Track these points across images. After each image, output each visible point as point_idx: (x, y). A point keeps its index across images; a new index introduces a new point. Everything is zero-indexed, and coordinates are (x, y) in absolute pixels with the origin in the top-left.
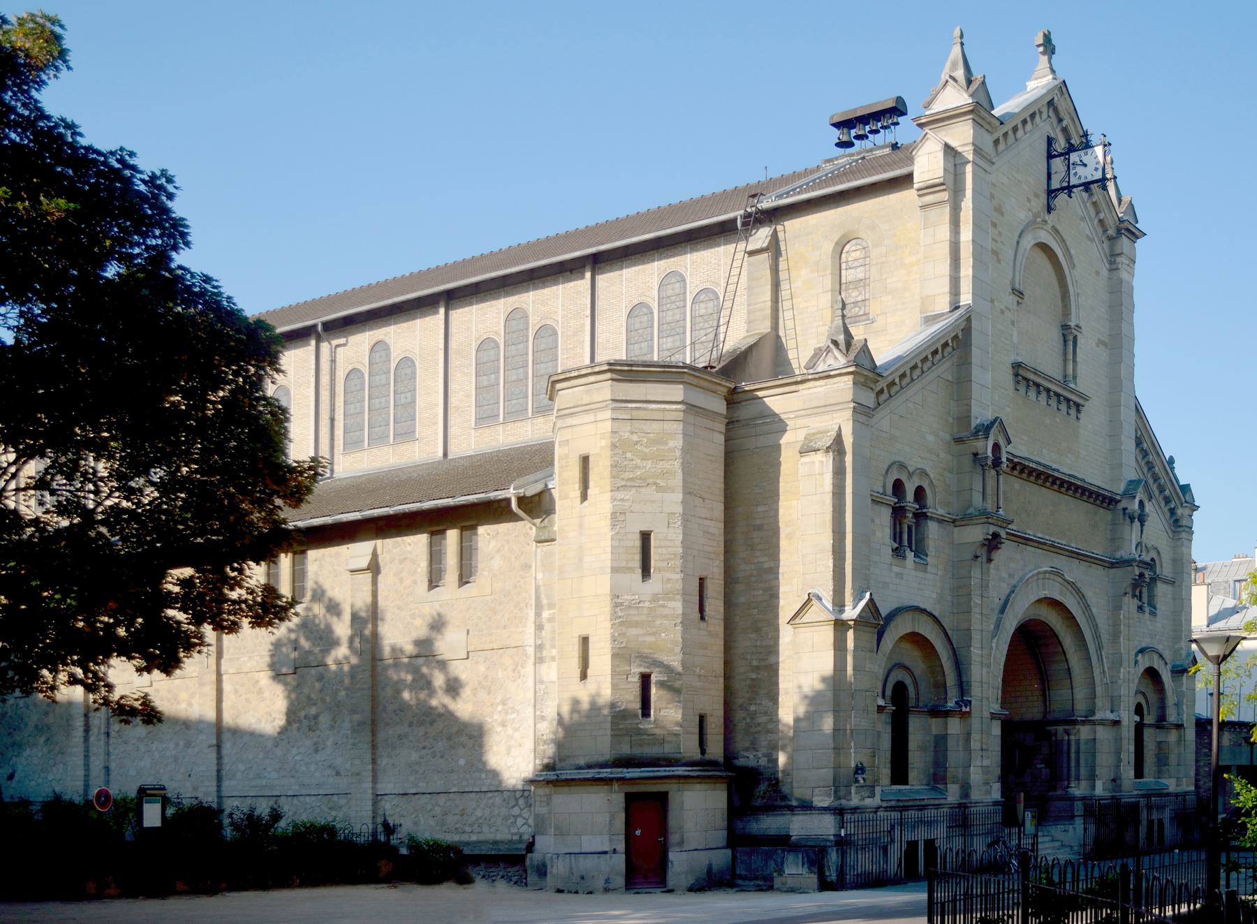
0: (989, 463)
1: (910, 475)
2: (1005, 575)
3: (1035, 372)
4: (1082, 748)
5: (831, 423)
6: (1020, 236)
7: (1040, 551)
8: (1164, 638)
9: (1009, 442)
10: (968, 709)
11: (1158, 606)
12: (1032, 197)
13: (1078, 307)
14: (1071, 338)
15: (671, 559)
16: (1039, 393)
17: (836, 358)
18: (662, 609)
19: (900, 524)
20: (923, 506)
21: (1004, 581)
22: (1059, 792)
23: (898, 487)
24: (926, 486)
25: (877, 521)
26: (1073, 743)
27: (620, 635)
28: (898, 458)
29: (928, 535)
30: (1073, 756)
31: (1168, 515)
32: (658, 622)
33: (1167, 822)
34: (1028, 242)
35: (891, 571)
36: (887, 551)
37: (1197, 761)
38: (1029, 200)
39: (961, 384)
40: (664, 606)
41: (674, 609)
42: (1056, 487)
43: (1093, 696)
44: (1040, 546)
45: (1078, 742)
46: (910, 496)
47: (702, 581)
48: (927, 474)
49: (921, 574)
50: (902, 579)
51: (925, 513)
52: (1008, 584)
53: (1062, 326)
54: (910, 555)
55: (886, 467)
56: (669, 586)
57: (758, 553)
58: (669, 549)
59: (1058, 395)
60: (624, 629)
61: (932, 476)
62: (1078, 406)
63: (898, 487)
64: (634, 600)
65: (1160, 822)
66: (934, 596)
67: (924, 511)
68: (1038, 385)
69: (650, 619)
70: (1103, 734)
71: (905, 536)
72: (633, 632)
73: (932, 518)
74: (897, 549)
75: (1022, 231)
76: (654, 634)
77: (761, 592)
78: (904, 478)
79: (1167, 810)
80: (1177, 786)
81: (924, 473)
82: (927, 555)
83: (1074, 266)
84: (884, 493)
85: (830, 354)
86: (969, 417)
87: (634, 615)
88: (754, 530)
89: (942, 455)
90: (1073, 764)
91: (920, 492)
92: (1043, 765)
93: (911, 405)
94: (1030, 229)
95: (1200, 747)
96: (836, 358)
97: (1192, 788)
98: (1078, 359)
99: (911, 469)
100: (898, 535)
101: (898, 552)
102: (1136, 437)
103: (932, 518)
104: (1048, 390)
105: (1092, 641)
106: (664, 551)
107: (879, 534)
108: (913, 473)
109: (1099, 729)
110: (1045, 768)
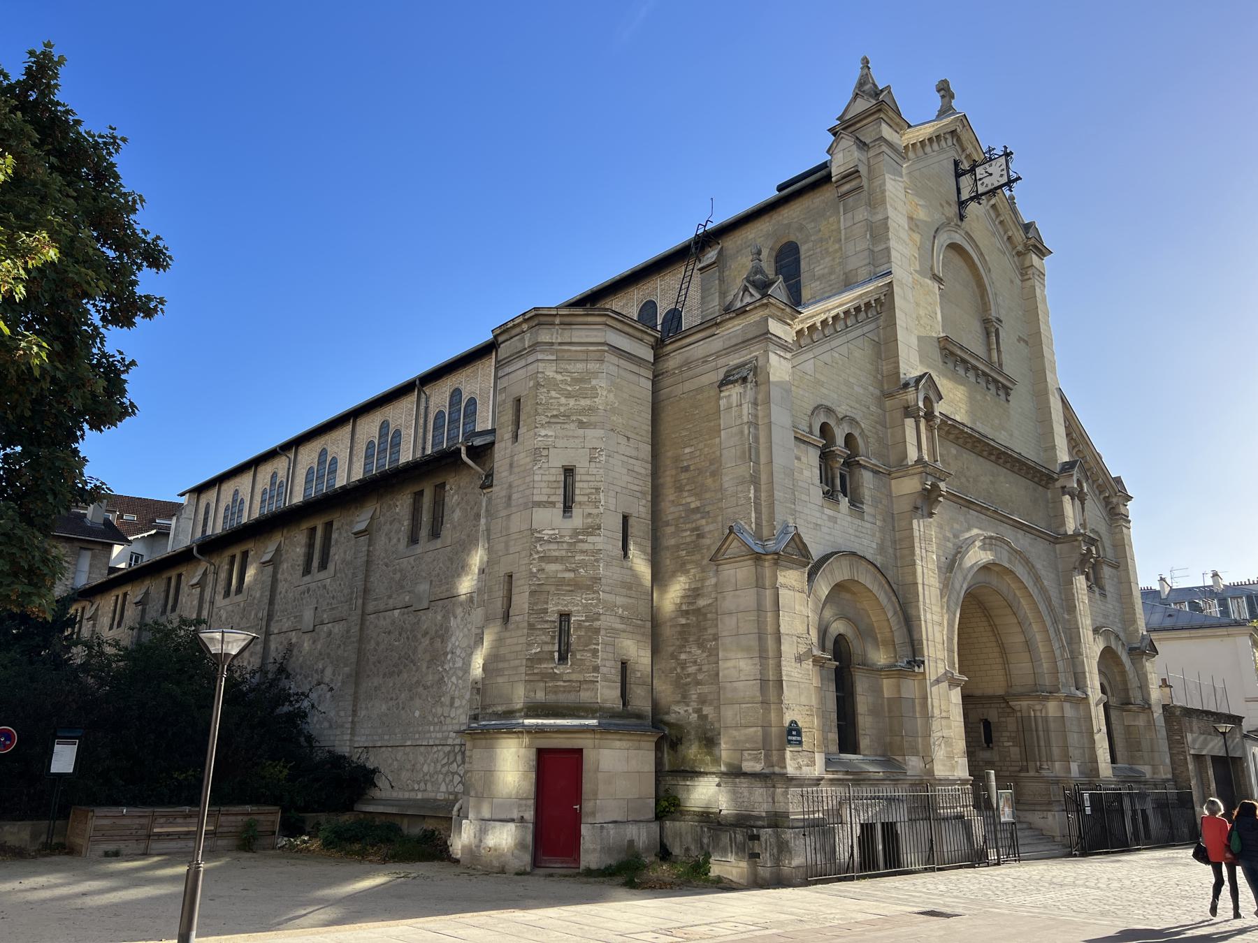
0: (921, 414)
2: (949, 535)
3: (962, 348)
4: (1052, 725)
5: (749, 357)
6: (936, 232)
7: (984, 517)
8: (1117, 620)
9: (941, 398)
10: (921, 670)
11: (1107, 588)
12: (945, 204)
13: (997, 304)
14: (993, 330)
15: (592, 494)
16: (967, 370)
17: (752, 295)
18: (580, 544)
19: (831, 470)
21: (949, 541)
22: (1032, 773)
23: (825, 430)
24: (856, 434)
25: (804, 459)
26: (1040, 720)
27: (539, 570)
30: (1041, 733)
31: (1104, 504)
32: (577, 558)
33: (1150, 812)
34: (944, 239)
35: (823, 513)
36: (817, 492)
37: (1170, 749)
38: (942, 206)
39: (885, 347)
40: (582, 541)
41: (594, 544)
42: (993, 458)
43: (1055, 672)
44: (983, 511)
45: (1046, 719)
46: (840, 441)
47: (625, 519)
48: (857, 422)
49: (858, 522)
50: (836, 523)
52: (954, 545)
54: (844, 502)
55: (811, 408)
56: (590, 520)
57: (686, 494)
58: (590, 483)
59: (985, 374)
60: (543, 565)
61: (863, 425)
62: (1006, 388)
63: (825, 430)
64: (554, 534)
65: (1143, 811)
66: (874, 546)
67: (857, 459)
68: (964, 361)
69: (570, 554)
70: (1069, 711)
71: (838, 482)
72: (552, 568)
73: (865, 467)
74: (828, 492)
75: (938, 229)
76: (573, 571)
77: (688, 533)
78: (832, 423)
79: (1149, 799)
80: (1154, 774)
81: (852, 421)
82: (862, 503)
83: (990, 271)
84: (811, 433)
85: (746, 293)
86: (898, 373)
87: (554, 550)
88: (682, 472)
89: (873, 408)
90: (1042, 743)
91: (849, 439)
92: (1011, 744)
93: (836, 355)
94: (945, 229)
95: (1171, 733)
96: (752, 295)
97: (1169, 776)
98: (1002, 349)
99: (840, 416)
100: (830, 480)
101: (830, 495)
103: (865, 467)
104: (975, 368)
105: (1047, 613)
106: (585, 485)
107: (807, 473)
108: (842, 419)
109: (1067, 706)
110: (1013, 746)
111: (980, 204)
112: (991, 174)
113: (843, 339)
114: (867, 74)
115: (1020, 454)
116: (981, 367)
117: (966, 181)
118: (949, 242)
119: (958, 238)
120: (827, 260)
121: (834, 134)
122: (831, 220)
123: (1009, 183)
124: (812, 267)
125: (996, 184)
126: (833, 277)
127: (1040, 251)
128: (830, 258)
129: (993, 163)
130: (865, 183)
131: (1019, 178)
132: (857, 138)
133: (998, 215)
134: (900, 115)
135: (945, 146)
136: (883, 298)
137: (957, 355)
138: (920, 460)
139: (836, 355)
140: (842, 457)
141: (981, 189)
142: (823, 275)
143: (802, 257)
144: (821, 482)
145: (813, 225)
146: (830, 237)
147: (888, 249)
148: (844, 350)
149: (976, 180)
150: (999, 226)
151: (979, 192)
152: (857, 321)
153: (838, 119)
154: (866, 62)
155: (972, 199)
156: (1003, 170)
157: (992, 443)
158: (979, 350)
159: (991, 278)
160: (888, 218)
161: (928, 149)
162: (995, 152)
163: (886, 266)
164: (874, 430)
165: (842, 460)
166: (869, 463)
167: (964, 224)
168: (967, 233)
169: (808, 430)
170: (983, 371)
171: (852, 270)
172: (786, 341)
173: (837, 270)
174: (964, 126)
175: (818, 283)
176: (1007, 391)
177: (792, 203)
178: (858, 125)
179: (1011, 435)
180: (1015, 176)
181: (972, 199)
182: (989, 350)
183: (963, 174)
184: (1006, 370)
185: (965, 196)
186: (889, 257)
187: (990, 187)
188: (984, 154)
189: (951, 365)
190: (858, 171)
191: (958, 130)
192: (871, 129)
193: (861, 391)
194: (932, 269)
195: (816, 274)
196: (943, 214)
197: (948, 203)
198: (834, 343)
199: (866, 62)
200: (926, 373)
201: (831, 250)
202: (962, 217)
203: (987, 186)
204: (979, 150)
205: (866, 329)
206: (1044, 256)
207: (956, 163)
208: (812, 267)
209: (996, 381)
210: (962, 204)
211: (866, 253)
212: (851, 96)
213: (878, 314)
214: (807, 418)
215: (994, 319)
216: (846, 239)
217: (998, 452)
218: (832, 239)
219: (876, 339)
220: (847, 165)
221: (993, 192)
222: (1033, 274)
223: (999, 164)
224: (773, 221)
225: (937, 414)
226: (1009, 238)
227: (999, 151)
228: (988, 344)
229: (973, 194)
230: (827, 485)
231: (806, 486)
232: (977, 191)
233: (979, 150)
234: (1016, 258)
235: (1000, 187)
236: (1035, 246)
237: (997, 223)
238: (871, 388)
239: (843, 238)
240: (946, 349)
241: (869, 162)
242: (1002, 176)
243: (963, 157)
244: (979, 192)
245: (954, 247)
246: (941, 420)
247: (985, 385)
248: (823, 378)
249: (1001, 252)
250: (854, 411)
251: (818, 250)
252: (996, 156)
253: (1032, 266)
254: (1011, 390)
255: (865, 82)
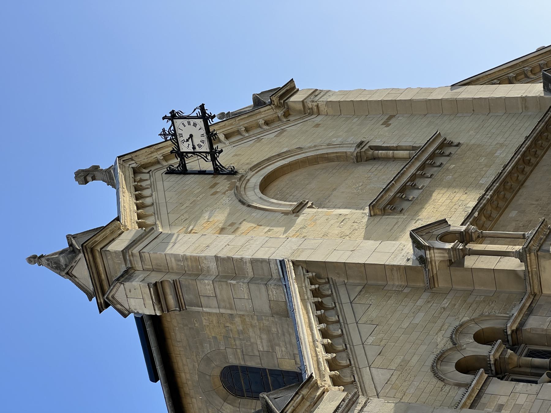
0: (461, 246)
1: (455, 345)
3: (386, 190)
6: (243, 203)
9: (444, 221)
12: (213, 190)
13: (341, 145)
14: (371, 152)
16: (414, 187)
20: (502, 334)
24: (476, 328)
25: (502, 400)
28: (429, 362)
29: (543, 330)
38: (216, 193)
46: (483, 350)
48: (461, 325)
51: (513, 331)
53: (357, 162)
55: (435, 380)
59: (422, 167)
61: (466, 319)
67: (509, 332)
68: (403, 189)
71: (537, 361)
73: (522, 324)
75: (240, 201)
78: (458, 357)
81: (459, 331)
84: (467, 386)
86: (406, 268)
89: (446, 303)
93: (371, 340)
94: (243, 193)
98: (395, 145)
99: (450, 345)
100: (534, 371)
102: (499, 84)
103: (522, 324)
104: (413, 177)
107: (522, 400)
108: (455, 344)
111: (222, 151)
112: (191, 136)
113: (352, 327)
114: (48, 260)
115: (527, 138)
116: (412, 170)
117: (192, 164)
118: (258, 190)
119: (256, 179)
120: (251, 334)
121: (107, 305)
122: (205, 322)
123: (205, 116)
124: (257, 353)
125: (203, 131)
126: (274, 330)
127: (287, 92)
128: (251, 330)
129: (178, 132)
130: (170, 278)
131: (202, 107)
132: (118, 280)
133: (238, 132)
134: (103, 228)
135: (148, 182)
136: (310, 274)
137: (394, 197)
138: (521, 256)
139: (371, 340)
140: (504, 351)
141: (205, 148)
142: (270, 341)
143: (243, 363)
144: (536, 382)
145: (207, 345)
146: (225, 327)
147: (254, 262)
148: (365, 329)
149: (193, 153)
150: (251, 133)
151: (208, 150)
152: (333, 309)
153: (90, 299)
154: (34, 259)
155: (214, 159)
156: (189, 123)
157: (509, 168)
158: (391, 171)
159: (310, 148)
160: (216, 257)
161: (148, 201)
162: (167, 129)
163: (273, 266)
164: (474, 306)
165: (509, 351)
166: (516, 318)
167: (241, 171)
168: (251, 169)
169: (463, 390)
170: (418, 169)
171: (270, 306)
172: (343, 400)
173: (266, 323)
174: (132, 159)
175: (277, 348)
176: (446, 144)
177: (176, 366)
178: (103, 276)
179: (502, 145)
180: (198, 111)
181: (214, 159)
182: (394, 159)
183: (184, 166)
184: (420, 142)
185: (208, 166)
186: (262, 261)
187: (205, 138)
188: (166, 141)
189: (405, 205)
190: (155, 284)
191: (134, 165)
192: (110, 262)
193: (421, 315)
194: (286, 213)
195: (266, 349)
196: (224, 193)
197: (212, 187)
198: (355, 338)
199: (34, 259)
200: (411, 235)
201: (241, 328)
202: (233, 173)
203: (203, 142)
204: (160, 146)
205: (344, 298)
206: (294, 87)
207: (171, 172)
208: (257, 353)
209: (433, 156)
210: (218, 171)
211: (252, 286)
212: (68, 281)
213: (329, 282)
214: (447, 388)
215: (358, 150)
216: (231, 309)
217: (521, 161)
218: (228, 324)
219: (359, 288)
220: (145, 296)
221: (211, 136)
222: (313, 101)
223: (181, 127)
224: (192, 393)
225: (463, 228)
226: (267, 123)
227: (167, 125)
228: (387, 159)
229: (209, 157)
230: (541, 375)
231: (538, 403)
232: (206, 153)
233: (160, 146)
234: (291, 118)
235: (207, 127)
236: (281, 97)
237: (247, 135)
238: (420, 302)
239: (229, 312)
240: (384, 209)
241: (148, 270)
242: (195, 125)
243: (165, 163)
244: (208, 150)
245: (264, 186)
246: (471, 224)
247: (435, 169)
248: (398, 361)
249: (281, 133)
250: (446, 327)
251: (238, 342)
252: (172, 128)
253: (303, 101)
254: (445, 139)
255: (55, 263)
